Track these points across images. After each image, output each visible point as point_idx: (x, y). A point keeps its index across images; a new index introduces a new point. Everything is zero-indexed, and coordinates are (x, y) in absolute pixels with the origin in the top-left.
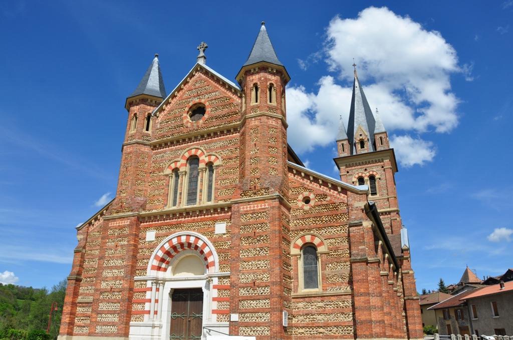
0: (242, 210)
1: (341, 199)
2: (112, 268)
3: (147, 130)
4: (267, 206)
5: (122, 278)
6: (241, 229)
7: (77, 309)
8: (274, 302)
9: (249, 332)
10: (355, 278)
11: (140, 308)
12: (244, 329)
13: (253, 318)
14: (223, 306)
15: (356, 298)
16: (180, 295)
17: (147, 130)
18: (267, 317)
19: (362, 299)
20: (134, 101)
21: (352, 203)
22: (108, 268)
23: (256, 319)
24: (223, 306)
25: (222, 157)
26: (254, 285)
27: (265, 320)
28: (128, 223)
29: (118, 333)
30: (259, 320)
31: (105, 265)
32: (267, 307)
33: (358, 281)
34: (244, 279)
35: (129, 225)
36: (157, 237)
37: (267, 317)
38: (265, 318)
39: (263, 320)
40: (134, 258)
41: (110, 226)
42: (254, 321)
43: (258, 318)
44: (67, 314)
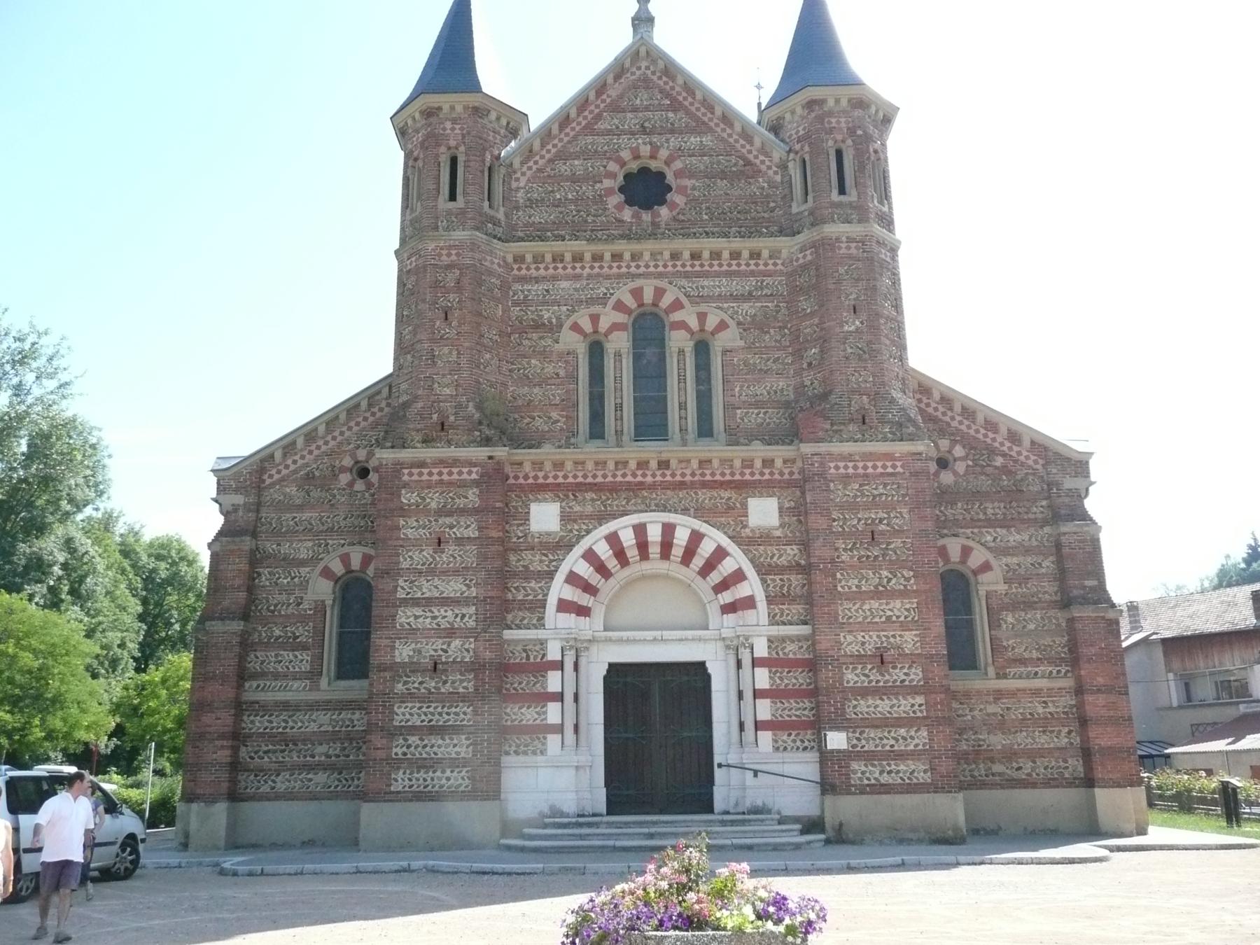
0: (832, 471)
1: (1030, 466)
2: (428, 602)
3: (842, 191)
4: (899, 470)
5: (467, 634)
6: (834, 520)
7: (393, 713)
8: (936, 704)
9: (877, 775)
10: (1085, 651)
11: (529, 717)
12: (863, 768)
13: (885, 741)
14: (787, 712)
15: (1089, 698)
16: (629, 679)
17: (842, 191)
18: (921, 738)
19: (1101, 699)
20: (446, 108)
21: (1057, 478)
22: (416, 602)
23: (893, 742)
24: (787, 712)
25: (739, 324)
26: (881, 659)
27: (917, 745)
28: (474, 476)
29: (474, 790)
30: (899, 747)
31: (401, 594)
32: (919, 714)
33: (1089, 661)
34: (851, 643)
35: (476, 483)
36: (566, 518)
37: (921, 738)
38: (916, 741)
39: (912, 747)
40: (503, 576)
41: (406, 478)
42: (888, 748)
43: (897, 740)
44: (222, 736)
